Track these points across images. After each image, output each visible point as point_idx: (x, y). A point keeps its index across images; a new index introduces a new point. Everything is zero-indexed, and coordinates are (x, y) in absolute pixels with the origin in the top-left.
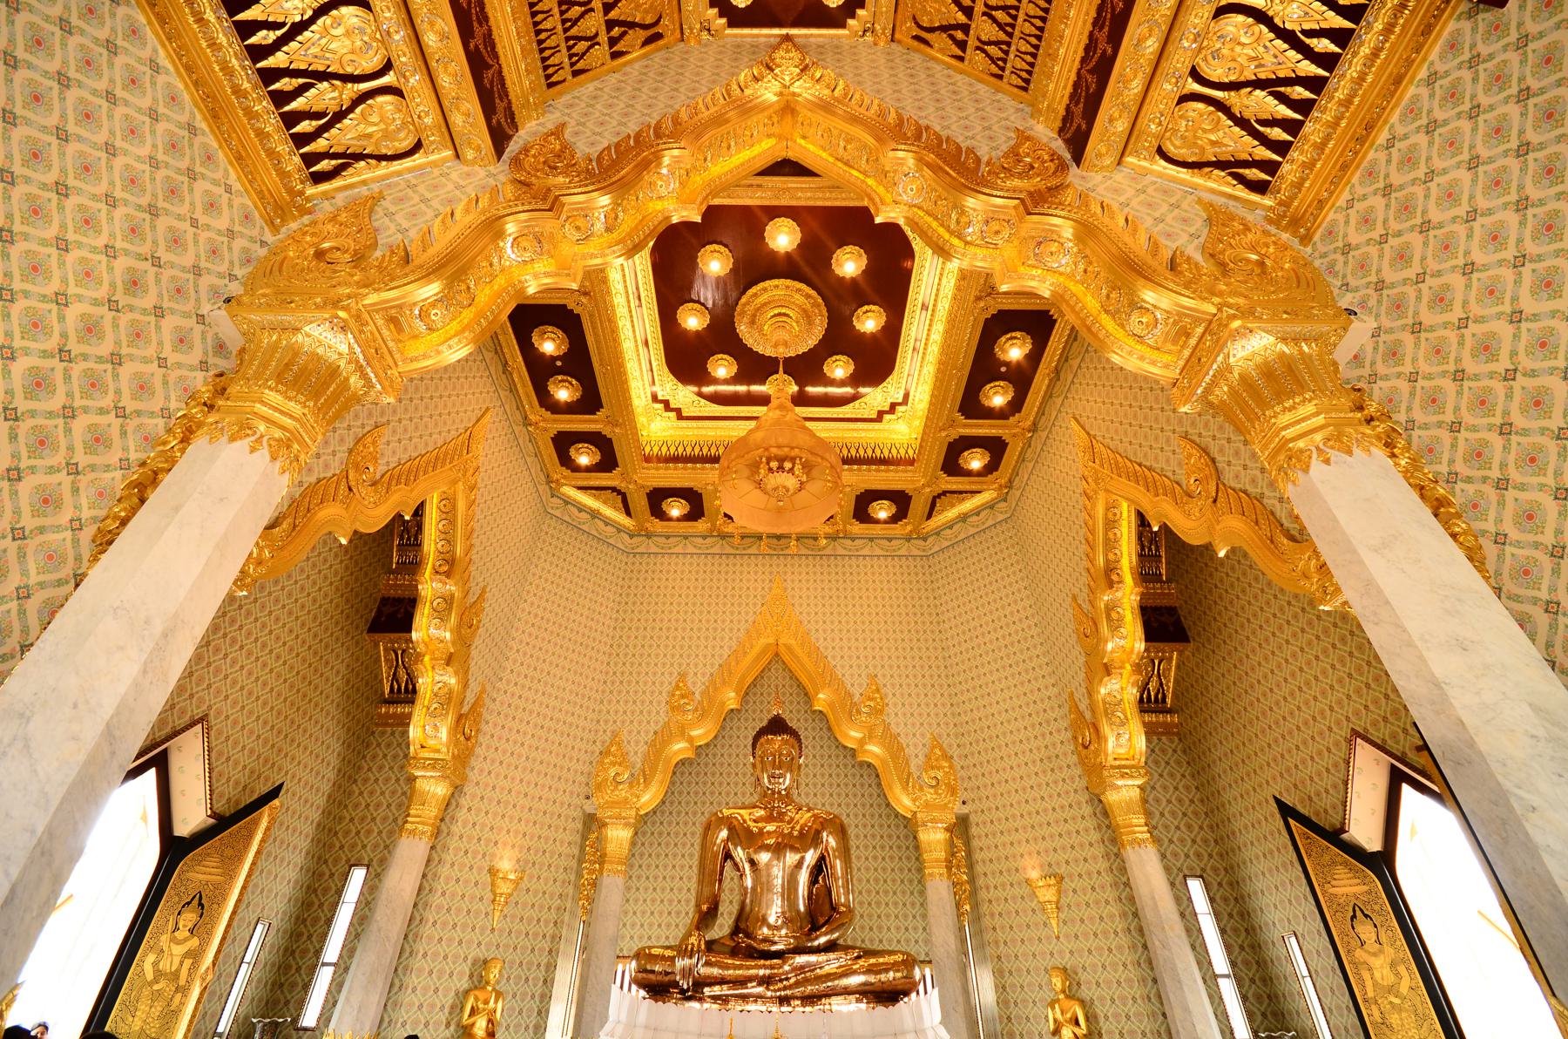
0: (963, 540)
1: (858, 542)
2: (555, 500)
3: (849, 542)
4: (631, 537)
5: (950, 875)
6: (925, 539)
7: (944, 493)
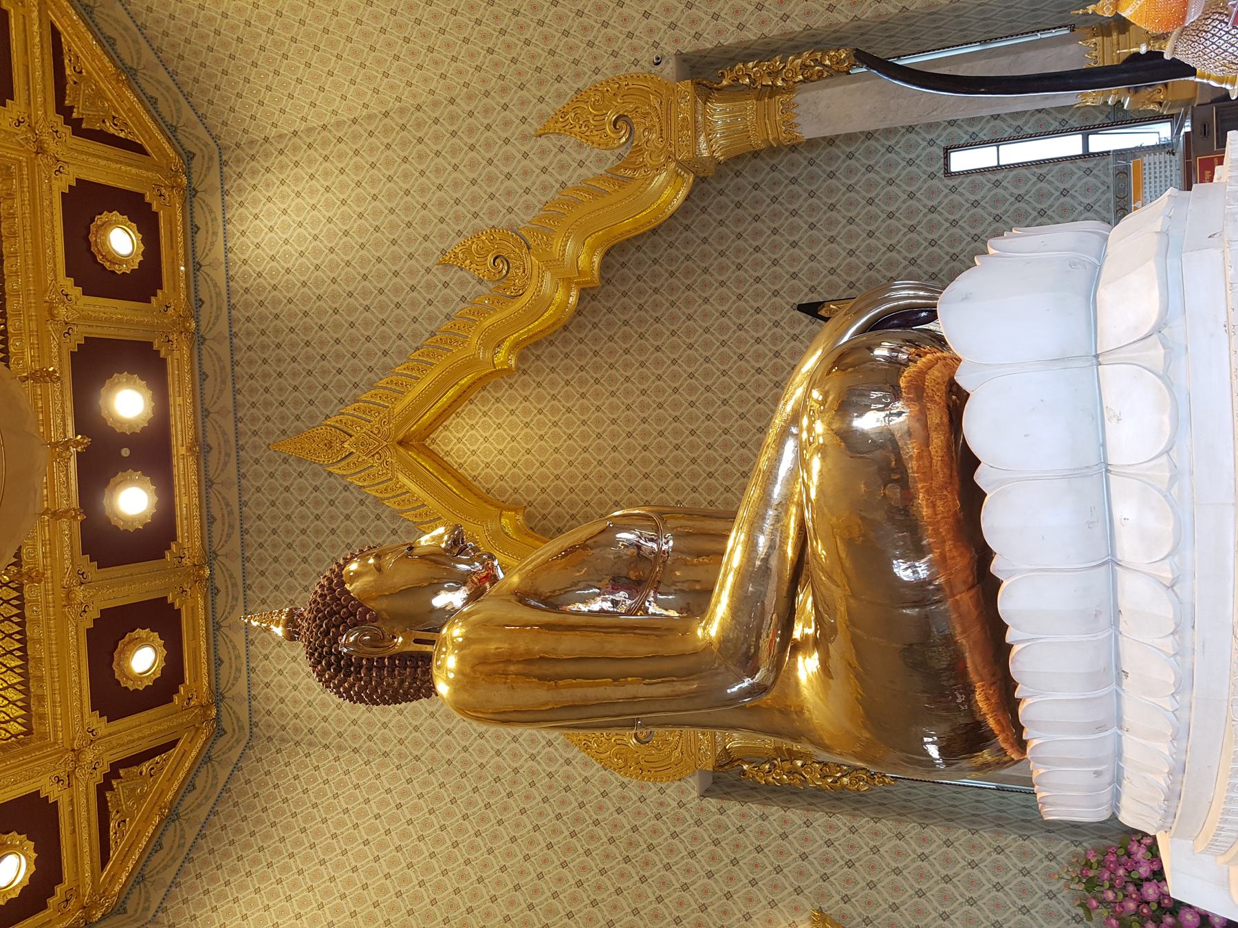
0: (172, 74)
1: (203, 295)
2: (130, 907)
3: (205, 310)
4: (221, 732)
5: (788, 90)
6: (191, 156)
7: (64, 110)
